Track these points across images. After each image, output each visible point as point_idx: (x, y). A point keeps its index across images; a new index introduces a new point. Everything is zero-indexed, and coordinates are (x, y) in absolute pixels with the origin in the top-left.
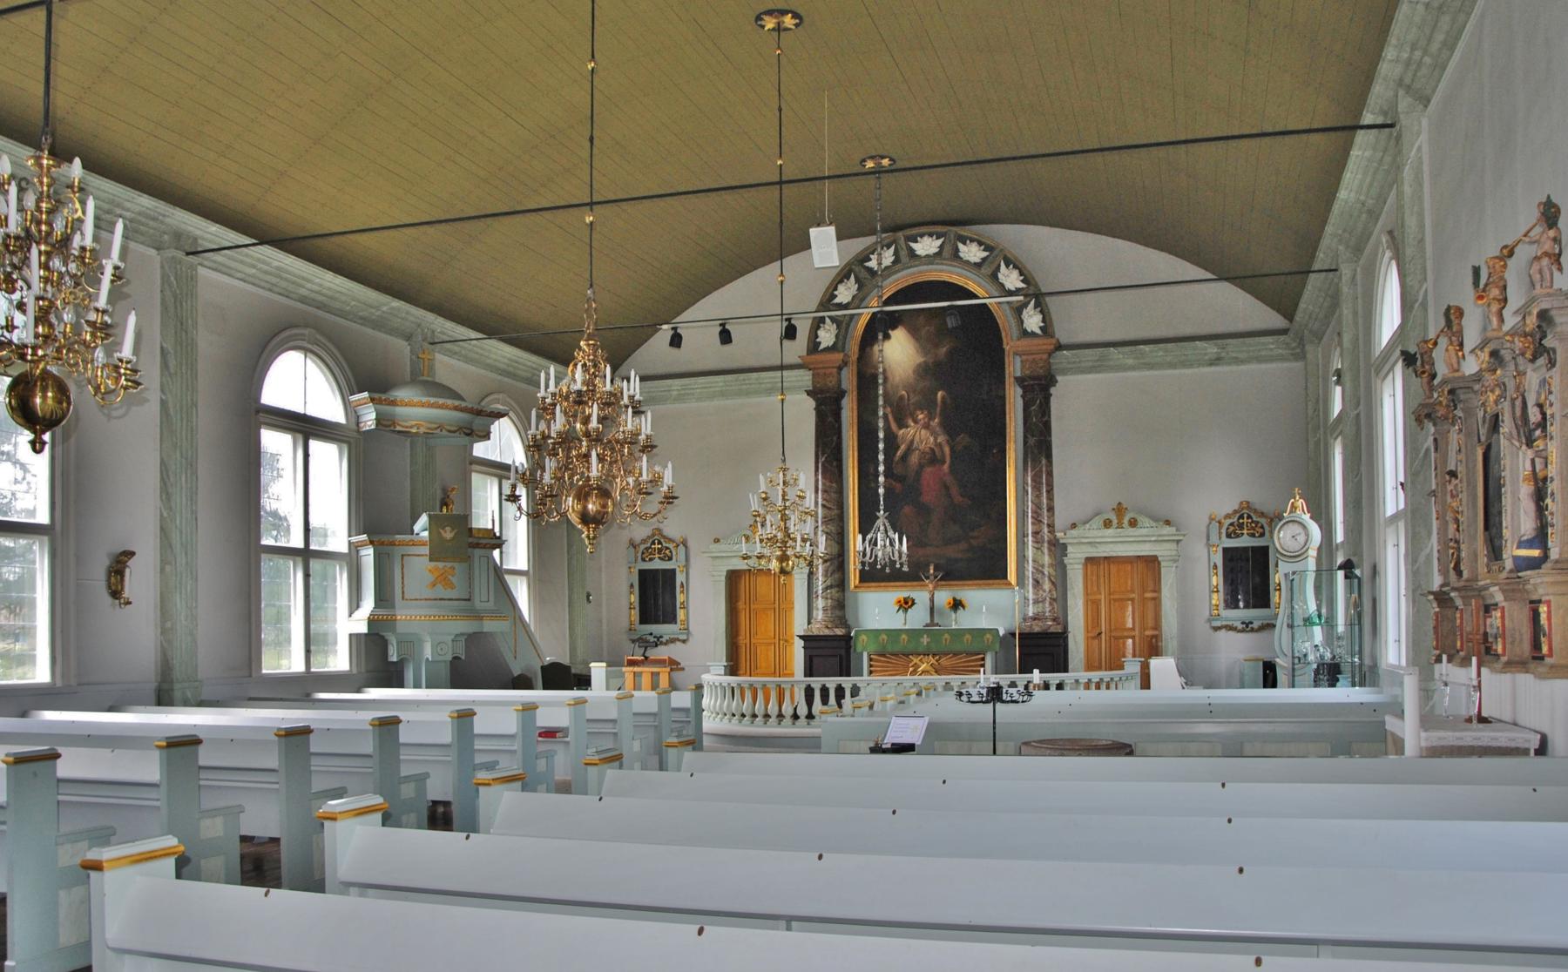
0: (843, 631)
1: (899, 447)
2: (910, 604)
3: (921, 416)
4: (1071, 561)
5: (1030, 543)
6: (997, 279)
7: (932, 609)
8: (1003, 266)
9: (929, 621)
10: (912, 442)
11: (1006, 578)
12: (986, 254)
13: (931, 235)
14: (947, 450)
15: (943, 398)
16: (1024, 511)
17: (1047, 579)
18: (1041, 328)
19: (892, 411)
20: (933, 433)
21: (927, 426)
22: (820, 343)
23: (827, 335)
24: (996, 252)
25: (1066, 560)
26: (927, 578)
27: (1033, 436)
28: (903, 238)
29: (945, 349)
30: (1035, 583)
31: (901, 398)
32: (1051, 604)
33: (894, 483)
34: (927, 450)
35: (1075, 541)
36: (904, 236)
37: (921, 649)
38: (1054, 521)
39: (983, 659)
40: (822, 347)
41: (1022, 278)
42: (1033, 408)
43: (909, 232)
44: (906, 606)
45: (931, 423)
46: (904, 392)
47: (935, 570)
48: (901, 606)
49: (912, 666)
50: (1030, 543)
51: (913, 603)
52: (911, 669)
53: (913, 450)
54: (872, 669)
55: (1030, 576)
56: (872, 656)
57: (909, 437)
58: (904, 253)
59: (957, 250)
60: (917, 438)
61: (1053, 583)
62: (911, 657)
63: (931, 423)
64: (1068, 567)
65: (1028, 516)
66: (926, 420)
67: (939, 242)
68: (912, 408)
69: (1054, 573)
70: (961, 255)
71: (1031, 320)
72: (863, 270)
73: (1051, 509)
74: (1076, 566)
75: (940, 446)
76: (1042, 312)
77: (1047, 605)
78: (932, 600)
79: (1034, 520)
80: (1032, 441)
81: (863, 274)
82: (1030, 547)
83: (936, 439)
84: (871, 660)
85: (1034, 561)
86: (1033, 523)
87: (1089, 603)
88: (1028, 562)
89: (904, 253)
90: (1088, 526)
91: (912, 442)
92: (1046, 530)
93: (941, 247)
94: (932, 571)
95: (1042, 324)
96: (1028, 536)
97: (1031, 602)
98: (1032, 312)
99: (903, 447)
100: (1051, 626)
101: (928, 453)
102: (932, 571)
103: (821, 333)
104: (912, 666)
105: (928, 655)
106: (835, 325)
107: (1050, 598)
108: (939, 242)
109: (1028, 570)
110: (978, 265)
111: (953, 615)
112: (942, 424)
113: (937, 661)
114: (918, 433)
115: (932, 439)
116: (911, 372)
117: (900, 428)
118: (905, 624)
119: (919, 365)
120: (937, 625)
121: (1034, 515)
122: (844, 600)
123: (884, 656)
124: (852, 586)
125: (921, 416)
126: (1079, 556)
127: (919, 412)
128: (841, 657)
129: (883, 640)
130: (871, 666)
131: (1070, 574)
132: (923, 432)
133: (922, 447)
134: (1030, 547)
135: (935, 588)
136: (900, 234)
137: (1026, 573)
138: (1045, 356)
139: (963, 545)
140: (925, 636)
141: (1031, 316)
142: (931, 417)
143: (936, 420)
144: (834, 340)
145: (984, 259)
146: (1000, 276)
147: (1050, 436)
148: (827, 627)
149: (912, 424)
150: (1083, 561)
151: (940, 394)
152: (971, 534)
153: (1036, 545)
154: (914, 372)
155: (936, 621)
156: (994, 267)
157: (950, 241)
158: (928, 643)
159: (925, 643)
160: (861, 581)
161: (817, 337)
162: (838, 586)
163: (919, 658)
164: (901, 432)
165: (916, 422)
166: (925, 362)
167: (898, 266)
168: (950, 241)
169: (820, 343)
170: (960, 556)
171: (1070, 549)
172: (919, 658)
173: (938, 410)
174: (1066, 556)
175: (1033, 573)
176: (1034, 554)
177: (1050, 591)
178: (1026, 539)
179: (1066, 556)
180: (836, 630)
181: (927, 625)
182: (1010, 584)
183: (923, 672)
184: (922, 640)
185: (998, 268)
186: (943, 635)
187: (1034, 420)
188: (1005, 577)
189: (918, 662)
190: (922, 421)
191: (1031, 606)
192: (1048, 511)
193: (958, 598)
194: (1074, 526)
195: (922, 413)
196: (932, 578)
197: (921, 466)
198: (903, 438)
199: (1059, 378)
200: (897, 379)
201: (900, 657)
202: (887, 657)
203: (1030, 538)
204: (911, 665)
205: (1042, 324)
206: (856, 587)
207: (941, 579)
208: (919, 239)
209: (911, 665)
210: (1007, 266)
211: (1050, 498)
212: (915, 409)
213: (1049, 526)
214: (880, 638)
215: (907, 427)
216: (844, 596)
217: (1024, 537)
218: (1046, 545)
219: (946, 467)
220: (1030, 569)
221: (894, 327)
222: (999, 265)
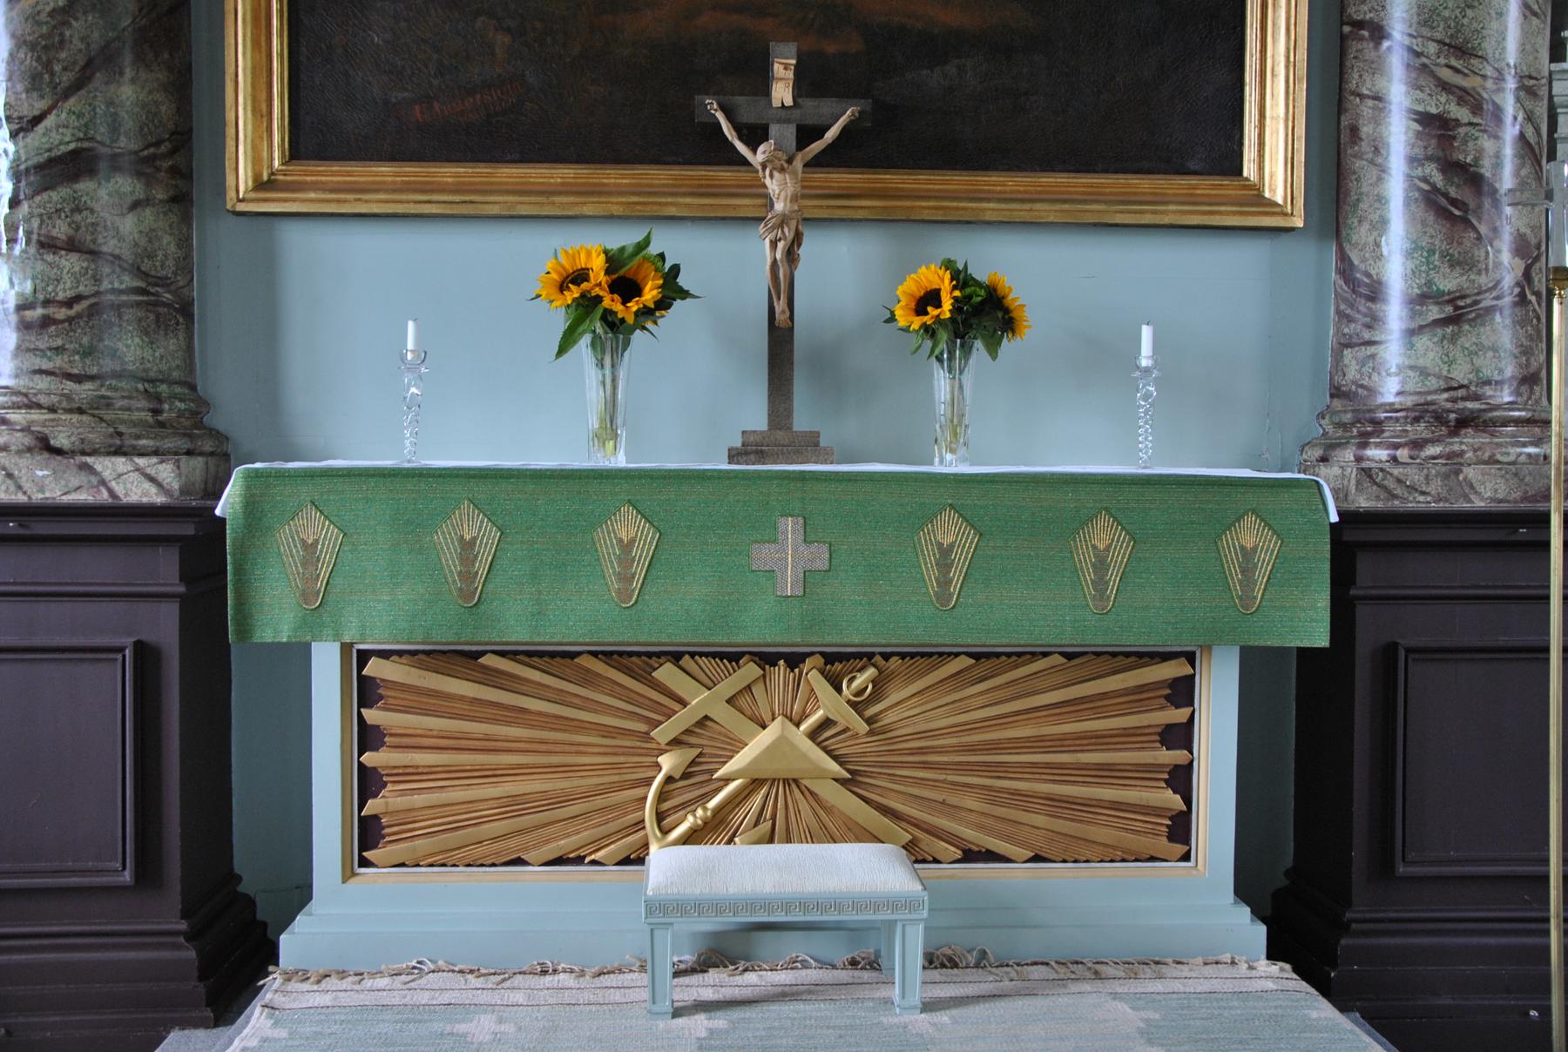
0: (166, 472)
2: (650, 294)
7: (780, 339)
9: (756, 417)
11: (1233, 166)
37: (757, 630)
39: (1182, 692)
44: (626, 311)
47: (805, 84)
48: (587, 304)
49: (676, 742)
51: (672, 292)
52: (667, 762)
54: (369, 758)
56: (373, 668)
62: (666, 673)
78: (782, 286)
84: (366, 692)
102: (782, 93)
104: (676, 742)
105: (794, 661)
111: (942, 382)
118: (609, 429)
120: (809, 445)
122: (185, 265)
123: (463, 659)
124: (241, 176)
128: (146, 655)
129: (468, 546)
130: (369, 737)
140: (790, 527)
148: (45, 446)
155: (802, 421)
158: (807, 577)
159: (790, 585)
160: (297, 151)
162: (143, 166)
163: (729, 686)
172: (729, 686)
180: (108, 466)
181: (749, 449)
182: (1256, 198)
184: (763, 555)
186: (927, 517)
189: (723, 714)
193: (980, 273)
196: (782, 133)
201: (589, 679)
202: (492, 678)
204: (663, 734)
206: (263, 185)
209: (663, 734)
214: (445, 541)
216: (185, 243)
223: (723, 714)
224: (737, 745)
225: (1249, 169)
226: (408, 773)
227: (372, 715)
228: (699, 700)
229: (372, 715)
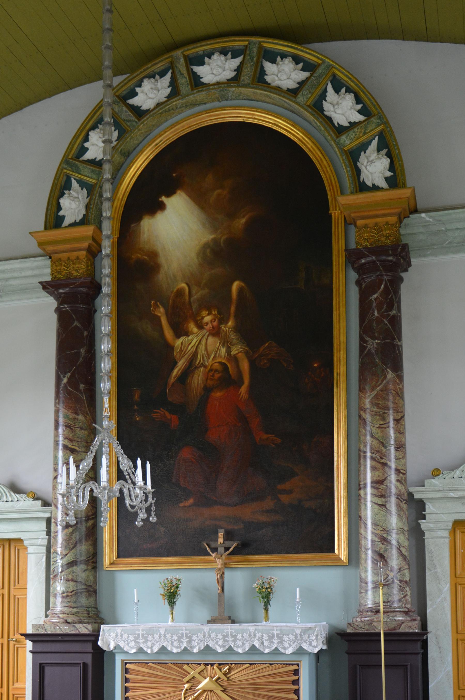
1: (175, 363)
3: (207, 319)
4: (432, 526)
5: (369, 498)
6: (321, 110)
8: (330, 88)
10: (195, 354)
12: (306, 75)
13: (224, 52)
14: (245, 365)
15: (240, 291)
16: (360, 450)
17: (394, 552)
18: (387, 179)
19: (167, 314)
20: (226, 343)
21: (216, 332)
22: (64, 217)
23: (74, 205)
24: (320, 70)
25: (424, 525)
26: (214, 550)
27: (374, 338)
28: (182, 60)
29: (243, 220)
30: (378, 558)
31: (180, 293)
32: (401, 589)
33: (168, 415)
34: (217, 366)
35: (438, 495)
36: (185, 57)
38: (405, 465)
40: (67, 222)
41: (359, 107)
42: (375, 296)
43: (199, 49)
45: (223, 327)
46: (184, 285)
49: (188, 682)
50: (369, 498)
52: (186, 686)
53: (197, 368)
55: (369, 546)
57: (191, 349)
58: (183, 82)
59: (263, 72)
60: (202, 350)
61: (404, 557)
62: (185, 667)
63: (223, 327)
64: (427, 535)
65: (365, 457)
66: (215, 324)
67: (236, 62)
68: (195, 306)
69: (406, 543)
70: (268, 78)
71: (371, 168)
72: (125, 108)
73: (400, 447)
74: (440, 534)
75: (235, 360)
76: (389, 155)
77: (395, 590)
79: (374, 463)
80: (372, 344)
81: (126, 114)
82: (369, 504)
83: (229, 350)
85: (375, 524)
86: (373, 468)
87: (459, 588)
88: (365, 524)
89: (183, 82)
90: (458, 473)
91: (195, 354)
92: (393, 477)
93: (239, 69)
94: (221, 540)
95: (389, 174)
96: (365, 487)
97: (370, 586)
98: (374, 156)
99: (181, 364)
100: (403, 622)
101: (216, 371)
103: (65, 202)
104: (188, 682)
105: (212, 665)
106: (85, 191)
107: (401, 581)
108: (236, 62)
109: (366, 538)
110: (293, 92)
112: (237, 329)
113: (225, 674)
114: (204, 342)
115: (223, 350)
116: (193, 255)
117: (178, 336)
119: (206, 246)
121: (377, 456)
125: (207, 319)
126: (444, 517)
127: (204, 313)
130: (127, 680)
131: (430, 544)
132: (211, 340)
133: (209, 362)
134: (369, 504)
135: (226, 565)
136: (178, 53)
137: (363, 542)
138: (393, 219)
139: (269, 503)
141: (372, 162)
142: (223, 320)
143: (230, 323)
144: (84, 212)
145: (302, 84)
146: (326, 105)
147: (400, 339)
149: (195, 330)
150: (450, 525)
151: (236, 285)
152: (279, 487)
153: (379, 501)
154: (198, 255)
156: (318, 91)
157: (252, 58)
161: (59, 208)
164: (178, 342)
165: (200, 326)
166: (215, 241)
167: (177, 102)
168: (252, 58)
169: (64, 217)
170: (264, 518)
171: (429, 508)
173: (233, 309)
174: (424, 517)
175: (373, 541)
176: (375, 515)
177: (400, 570)
178: (362, 492)
179: (424, 517)
183: (204, 691)
185: (323, 96)
187: (376, 314)
188: (330, 548)
189: (197, 676)
190: (210, 326)
191: (370, 593)
192: (397, 449)
194: (436, 473)
195: (209, 314)
197: (208, 390)
198: (181, 350)
199: (414, 261)
200: (175, 266)
201: (170, 668)
202: (151, 668)
203: (369, 490)
205: (389, 174)
207: (232, 554)
208: (206, 59)
210: (337, 91)
211: (400, 432)
212: (200, 309)
213: (398, 471)
215: (187, 334)
217: (360, 489)
218: (393, 500)
219: (244, 389)
220: (370, 537)
221: (170, 193)
222: (325, 91)
223: (197, 676)
224: (200, 683)
225: (336, 551)
226: (134, 688)
227: (127, 676)
228: (192, 672)
229: (127, 676)
